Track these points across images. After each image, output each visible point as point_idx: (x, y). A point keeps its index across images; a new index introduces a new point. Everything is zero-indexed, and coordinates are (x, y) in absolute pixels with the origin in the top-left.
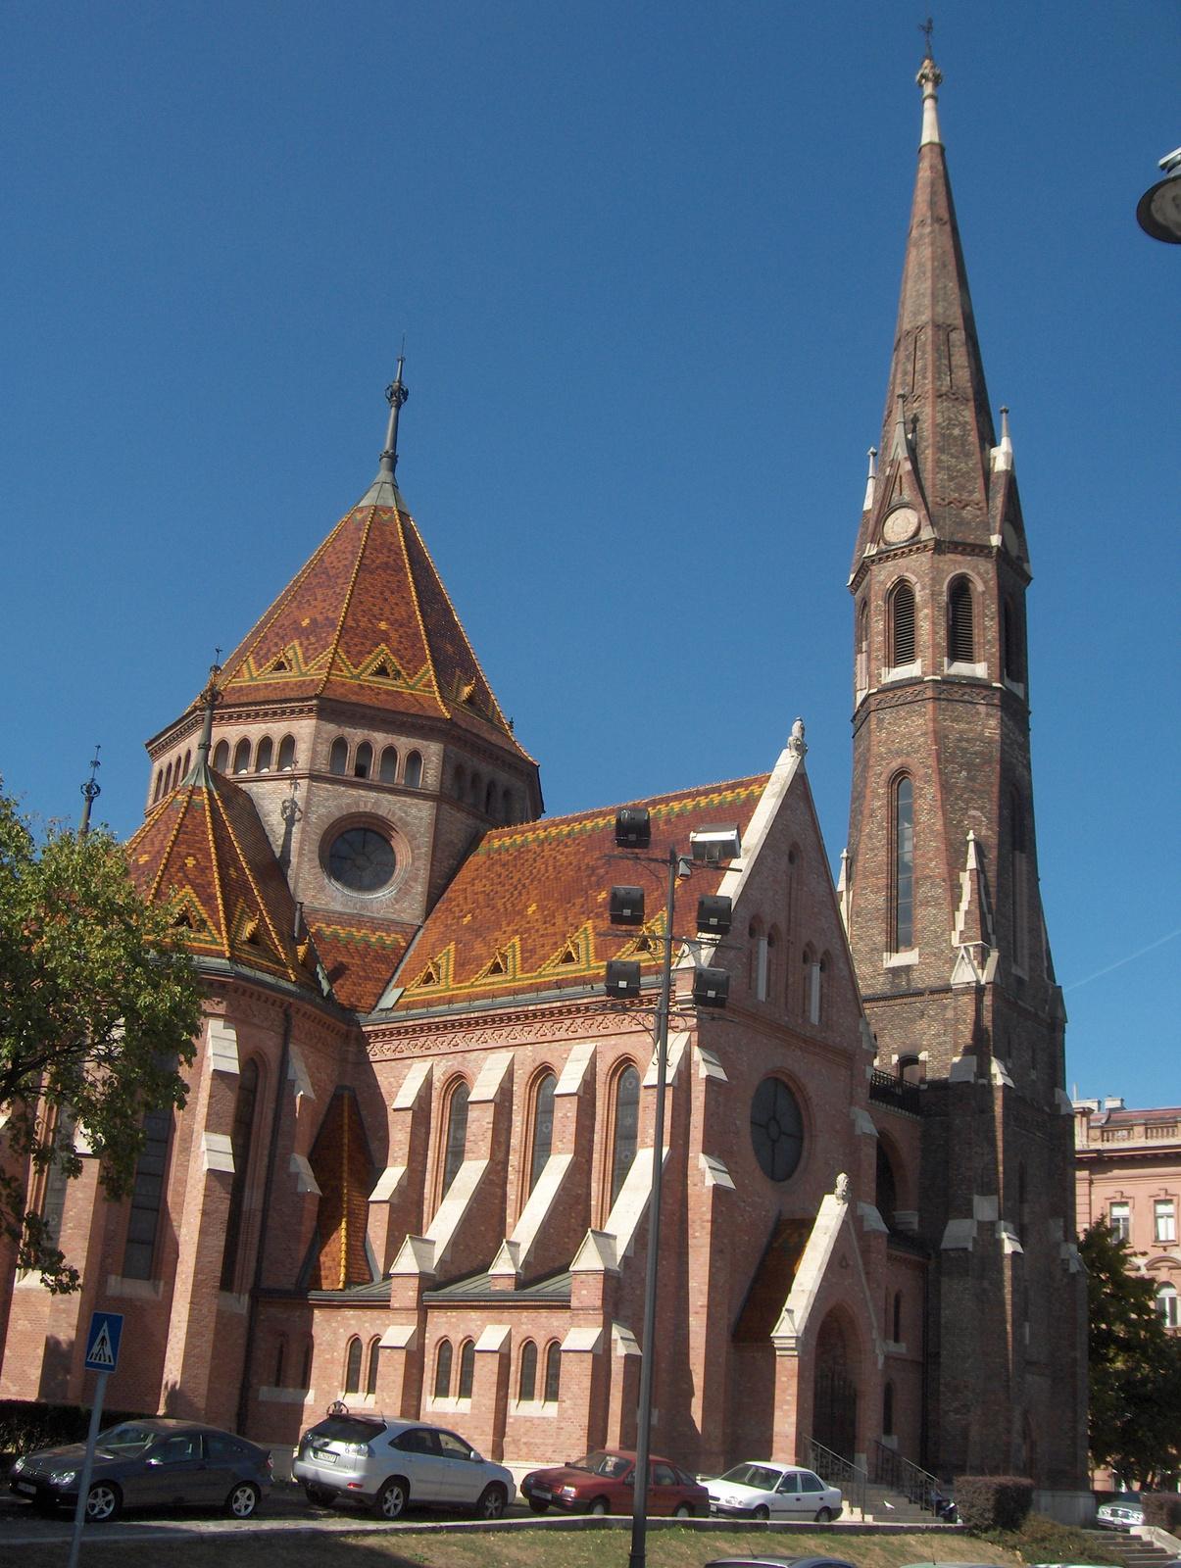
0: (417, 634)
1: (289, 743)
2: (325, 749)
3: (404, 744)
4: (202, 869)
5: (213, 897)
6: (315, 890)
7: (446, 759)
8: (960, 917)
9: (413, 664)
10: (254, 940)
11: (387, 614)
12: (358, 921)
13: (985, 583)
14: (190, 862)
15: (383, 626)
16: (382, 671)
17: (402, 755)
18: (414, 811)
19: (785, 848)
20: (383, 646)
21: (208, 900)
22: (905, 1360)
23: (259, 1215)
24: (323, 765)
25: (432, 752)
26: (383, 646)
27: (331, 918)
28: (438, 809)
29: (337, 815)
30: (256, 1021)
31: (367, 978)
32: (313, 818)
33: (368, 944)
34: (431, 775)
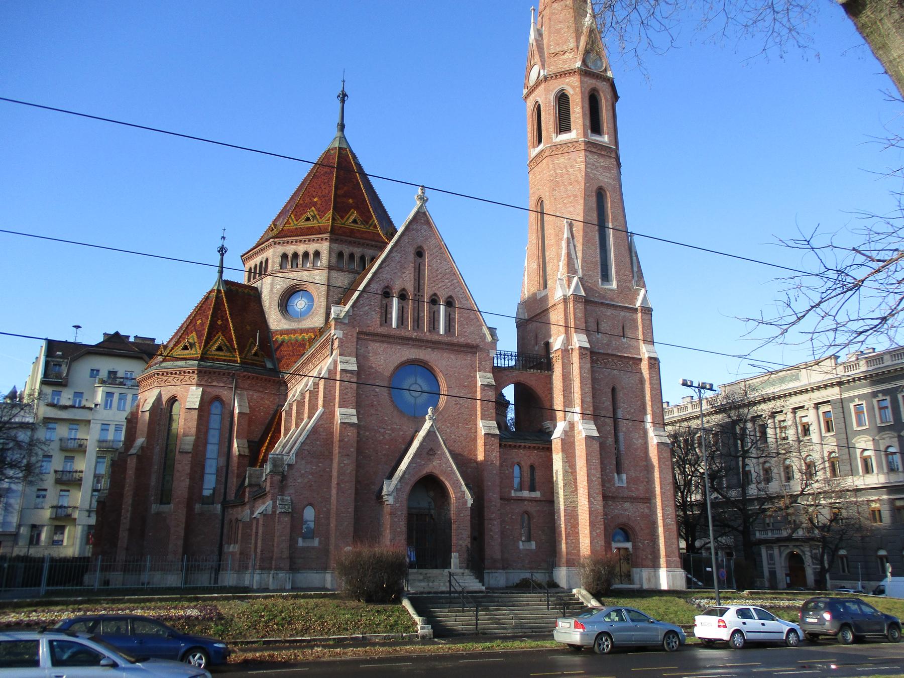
0: (330, 199)
1: (267, 260)
2: (278, 260)
3: (311, 248)
4: (202, 324)
5: (202, 335)
6: (276, 321)
7: (331, 251)
8: (561, 264)
9: (322, 213)
10: (219, 349)
11: (319, 194)
12: (294, 331)
13: (573, 88)
14: (199, 322)
15: (316, 199)
16: (308, 219)
17: (311, 253)
18: (318, 277)
19: (411, 250)
20: (313, 208)
21: (199, 337)
22: (536, 501)
23: (225, 469)
24: (278, 267)
25: (324, 247)
26: (313, 208)
27: (282, 332)
28: (329, 273)
29: (285, 287)
30: (215, 384)
31: (293, 355)
32: (275, 291)
33: (297, 340)
34: (324, 260)
